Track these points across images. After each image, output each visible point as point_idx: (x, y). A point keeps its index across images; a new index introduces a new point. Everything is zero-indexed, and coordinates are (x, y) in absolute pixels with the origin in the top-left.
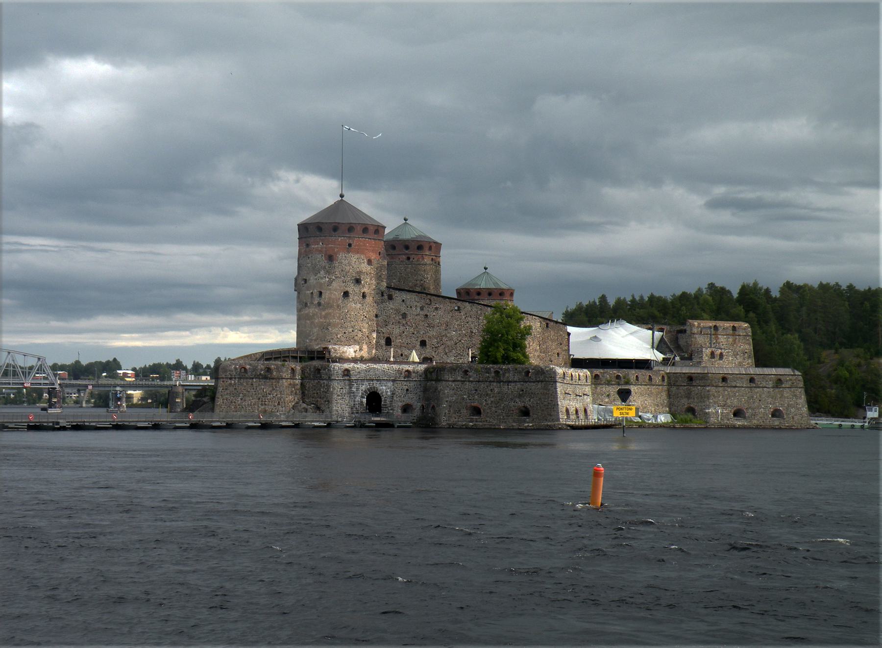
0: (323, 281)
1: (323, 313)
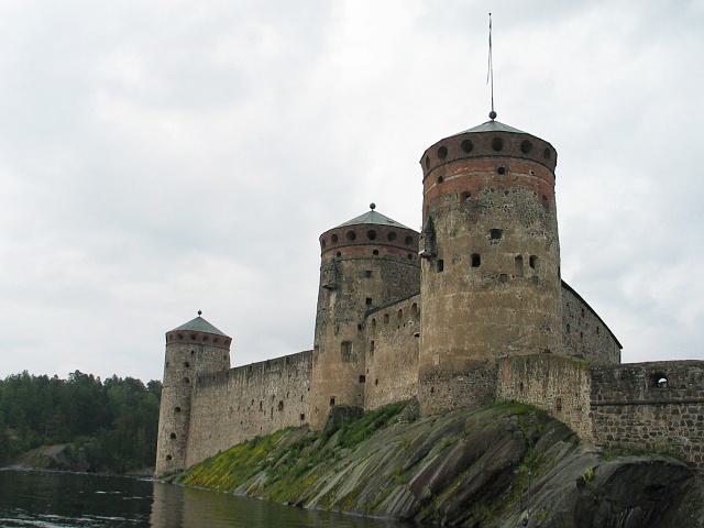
0: (539, 239)
1: (542, 298)
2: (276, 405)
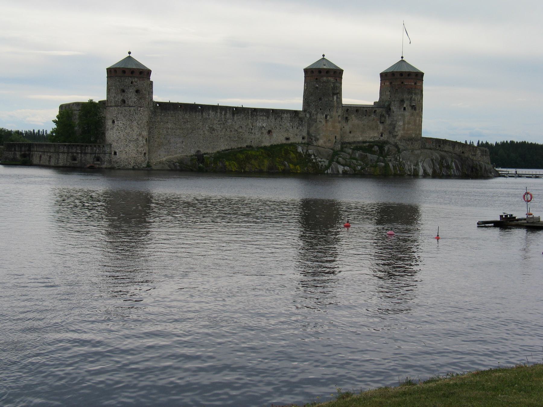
2: (265, 132)
